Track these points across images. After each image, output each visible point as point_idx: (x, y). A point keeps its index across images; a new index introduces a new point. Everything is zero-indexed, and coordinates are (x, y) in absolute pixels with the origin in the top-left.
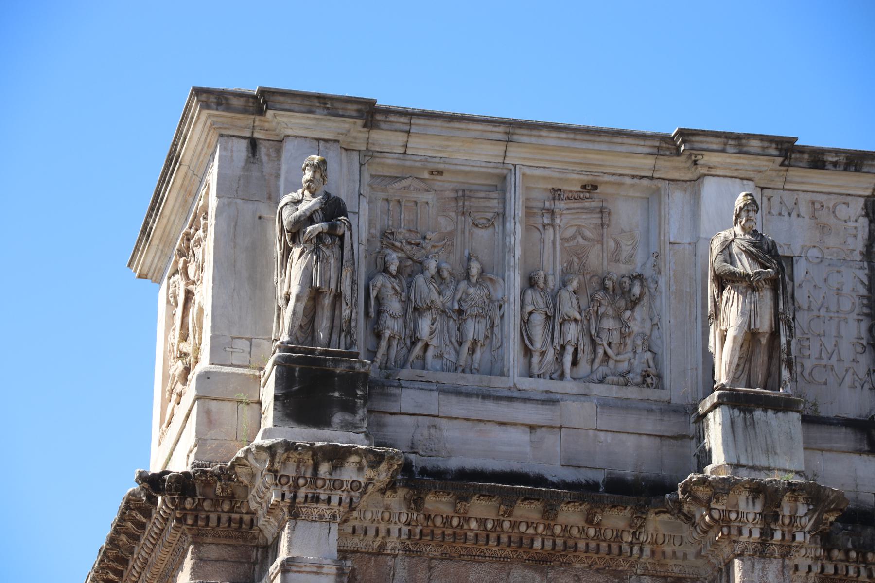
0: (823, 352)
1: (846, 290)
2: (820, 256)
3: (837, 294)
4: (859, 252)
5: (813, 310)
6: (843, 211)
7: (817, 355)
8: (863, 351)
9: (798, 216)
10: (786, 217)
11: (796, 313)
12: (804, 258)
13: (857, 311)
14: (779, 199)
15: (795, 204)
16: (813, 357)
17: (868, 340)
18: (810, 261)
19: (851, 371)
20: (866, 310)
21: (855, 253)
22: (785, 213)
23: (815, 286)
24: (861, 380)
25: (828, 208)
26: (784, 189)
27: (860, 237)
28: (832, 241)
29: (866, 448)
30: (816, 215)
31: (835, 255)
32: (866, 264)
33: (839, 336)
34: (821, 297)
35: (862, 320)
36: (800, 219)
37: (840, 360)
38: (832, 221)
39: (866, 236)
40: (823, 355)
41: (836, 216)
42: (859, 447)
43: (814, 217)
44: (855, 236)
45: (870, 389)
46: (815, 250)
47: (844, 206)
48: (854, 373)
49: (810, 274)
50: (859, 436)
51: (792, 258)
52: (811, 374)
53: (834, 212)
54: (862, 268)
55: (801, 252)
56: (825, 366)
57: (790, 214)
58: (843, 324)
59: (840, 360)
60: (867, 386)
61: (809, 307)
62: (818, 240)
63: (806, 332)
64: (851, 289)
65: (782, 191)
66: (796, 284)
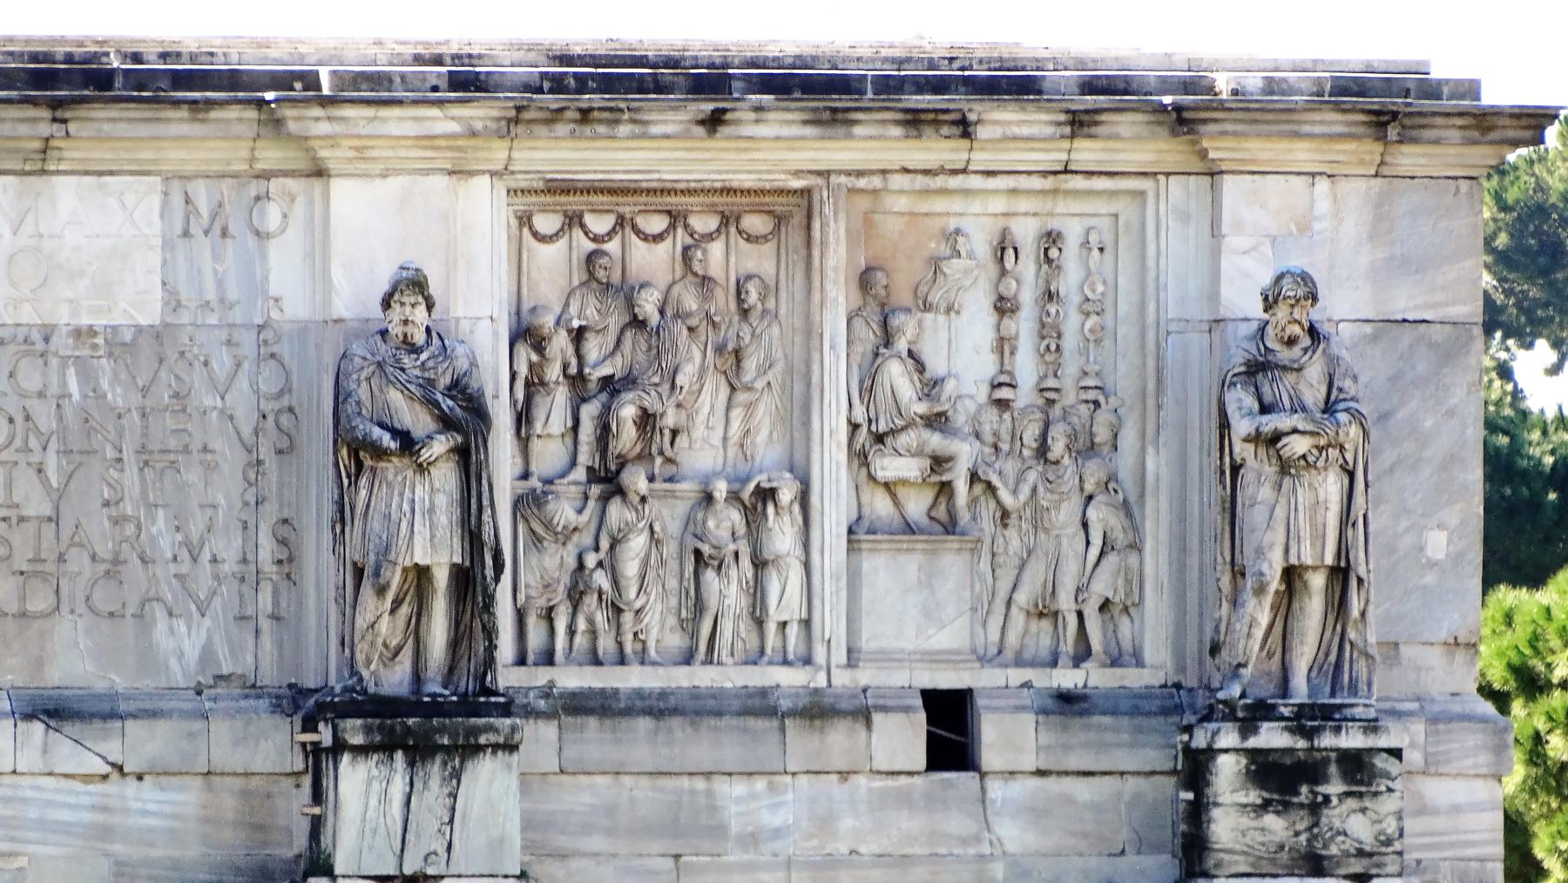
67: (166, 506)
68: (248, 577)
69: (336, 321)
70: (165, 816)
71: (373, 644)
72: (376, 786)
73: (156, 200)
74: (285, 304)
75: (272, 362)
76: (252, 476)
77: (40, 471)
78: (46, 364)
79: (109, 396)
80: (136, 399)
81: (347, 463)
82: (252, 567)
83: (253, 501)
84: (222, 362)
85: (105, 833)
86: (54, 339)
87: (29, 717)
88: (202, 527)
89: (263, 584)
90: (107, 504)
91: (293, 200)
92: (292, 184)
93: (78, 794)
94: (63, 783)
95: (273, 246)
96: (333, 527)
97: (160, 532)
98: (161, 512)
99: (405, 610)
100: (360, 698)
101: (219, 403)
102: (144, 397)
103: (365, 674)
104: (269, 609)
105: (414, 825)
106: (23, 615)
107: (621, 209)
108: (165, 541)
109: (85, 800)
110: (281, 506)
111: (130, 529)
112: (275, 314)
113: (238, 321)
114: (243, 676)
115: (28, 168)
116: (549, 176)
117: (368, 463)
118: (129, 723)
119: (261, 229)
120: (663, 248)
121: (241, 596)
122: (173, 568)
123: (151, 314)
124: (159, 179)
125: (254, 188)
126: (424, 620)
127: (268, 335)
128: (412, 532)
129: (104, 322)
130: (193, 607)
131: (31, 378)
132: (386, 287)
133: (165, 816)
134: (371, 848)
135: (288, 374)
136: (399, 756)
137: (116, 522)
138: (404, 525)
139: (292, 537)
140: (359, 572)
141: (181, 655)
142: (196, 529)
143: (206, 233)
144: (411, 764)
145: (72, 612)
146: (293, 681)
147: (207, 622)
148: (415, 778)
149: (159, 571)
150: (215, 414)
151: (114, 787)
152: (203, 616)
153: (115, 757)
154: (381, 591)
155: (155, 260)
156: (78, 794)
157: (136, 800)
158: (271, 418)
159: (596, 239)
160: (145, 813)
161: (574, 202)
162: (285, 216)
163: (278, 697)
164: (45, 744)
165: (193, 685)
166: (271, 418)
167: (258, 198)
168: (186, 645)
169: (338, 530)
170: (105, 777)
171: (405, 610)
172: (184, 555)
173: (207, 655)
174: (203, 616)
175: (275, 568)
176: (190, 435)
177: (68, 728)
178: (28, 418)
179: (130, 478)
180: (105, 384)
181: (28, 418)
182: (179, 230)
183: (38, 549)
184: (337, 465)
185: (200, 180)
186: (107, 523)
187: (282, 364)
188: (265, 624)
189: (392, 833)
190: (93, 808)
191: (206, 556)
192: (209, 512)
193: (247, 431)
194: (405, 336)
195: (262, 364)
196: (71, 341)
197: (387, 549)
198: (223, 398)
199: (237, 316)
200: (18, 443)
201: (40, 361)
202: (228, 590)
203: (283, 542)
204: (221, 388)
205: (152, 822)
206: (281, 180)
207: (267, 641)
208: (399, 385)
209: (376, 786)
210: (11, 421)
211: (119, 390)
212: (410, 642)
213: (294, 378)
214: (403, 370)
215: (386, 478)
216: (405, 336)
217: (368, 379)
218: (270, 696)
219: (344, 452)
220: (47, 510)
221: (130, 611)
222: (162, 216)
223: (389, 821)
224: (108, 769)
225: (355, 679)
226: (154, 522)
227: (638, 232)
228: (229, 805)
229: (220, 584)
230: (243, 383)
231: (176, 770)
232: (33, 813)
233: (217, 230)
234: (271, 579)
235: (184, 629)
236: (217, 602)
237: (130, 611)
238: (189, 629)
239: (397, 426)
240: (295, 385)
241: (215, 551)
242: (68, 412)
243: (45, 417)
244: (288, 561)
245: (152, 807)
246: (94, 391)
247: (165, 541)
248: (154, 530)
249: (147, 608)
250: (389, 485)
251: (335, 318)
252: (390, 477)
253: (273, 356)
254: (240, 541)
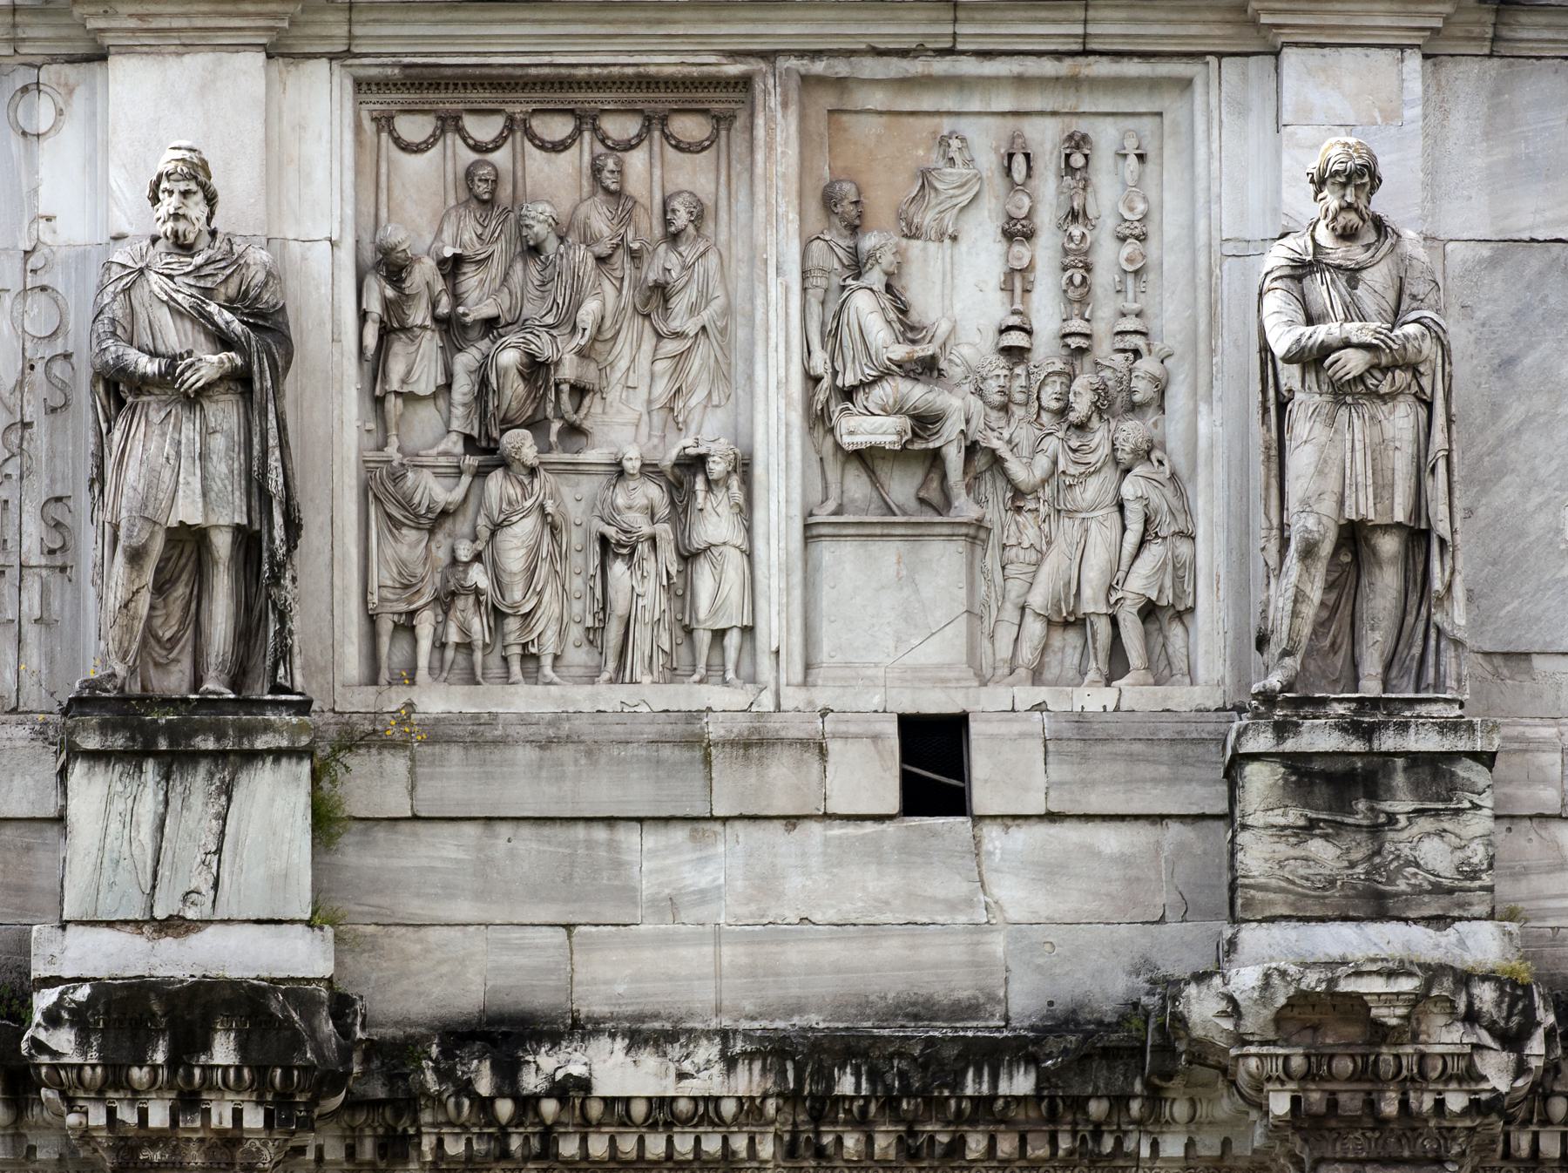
91: (71, 92)
107: (509, 108)
112: (46, 237)
116: (407, 60)
120: (566, 159)
127: (34, 261)
158: (40, 367)
159: (477, 148)
161: (449, 101)
166: (40, 367)
167: (25, 89)
188: (31, 633)
212: (189, 633)
227: (532, 137)
240: (71, 326)
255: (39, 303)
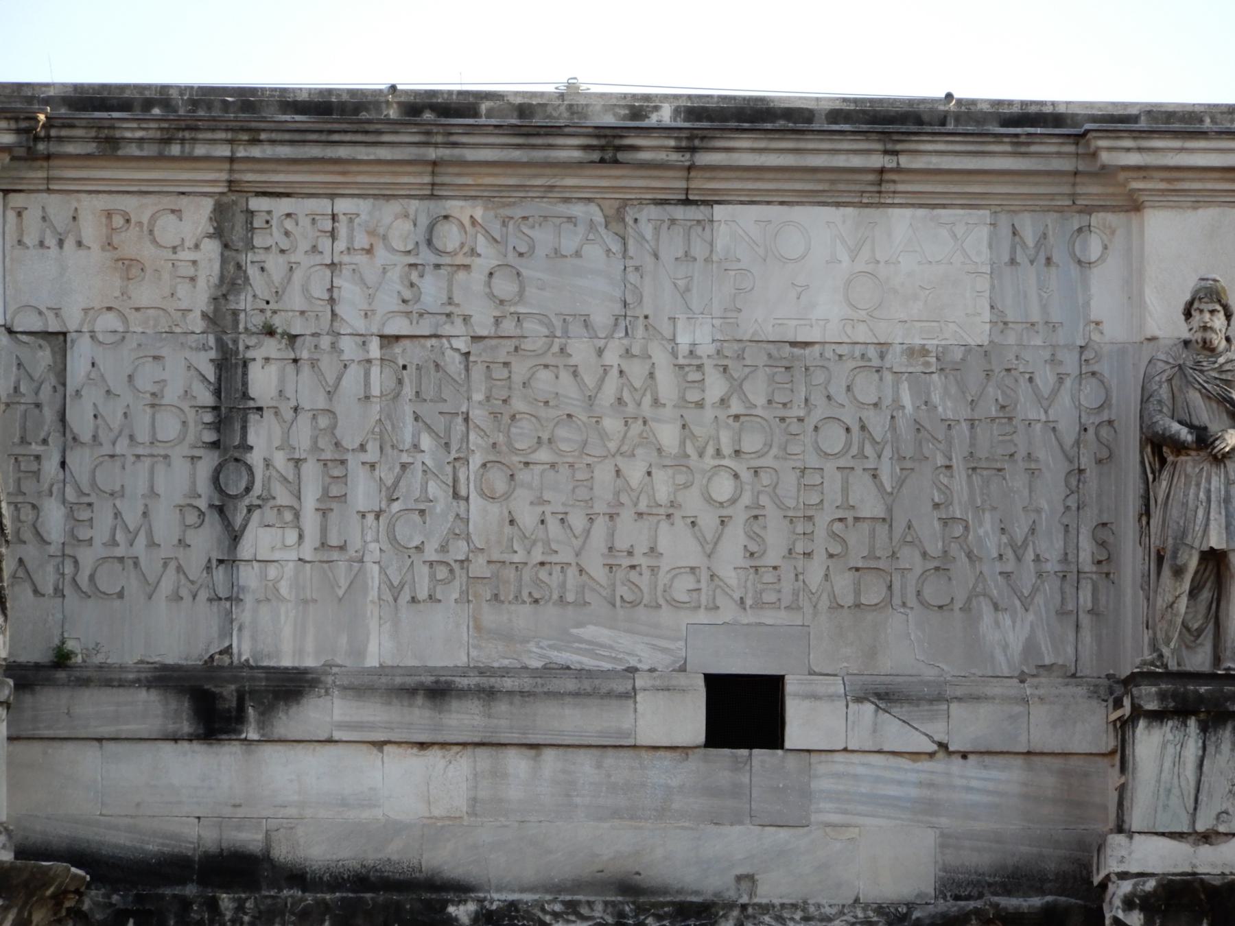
0: (118, 532)
1: (171, 395)
2: (121, 329)
3: (153, 406)
4: (199, 314)
5: (101, 444)
6: (169, 230)
7: (106, 537)
8: (199, 521)
9: (79, 244)
10: (54, 250)
11: (68, 453)
12: (88, 335)
13: (191, 437)
14: (40, 213)
15: (74, 218)
16: (97, 542)
17: (210, 498)
18: (100, 342)
19: (172, 565)
20: (210, 436)
21: (191, 316)
22: (51, 241)
23: (108, 392)
24: (192, 582)
25: (140, 224)
26: (48, 190)
27: (202, 283)
28: (145, 294)
29: (186, 728)
30: (116, 241)
31: (151, 323)
32: (211, 340)
33: (153, 493)
34: (120, 415)
35: (200, 458)
36: (82, 253)
37: (152, 544)
38: (147, 252)
39: (215, 280)
40: (118, 537)
41: (154, 241)
42: (171, 727)
43: (109, 245)
44: (193, 279)
45: (210, 600)
46: (111, 316)
47: (172, 217)
48: (179, 569)
49: (99, 369)
50: (173, 705)
51: (65, 334)
52: (92, 577)
53: (151, 232)
54: (205, 348)
55: (82, 324)
56: (121, 559)
57: (61, 243)
58: (160, 469)
59: (152, 544)
60: (203, 595)
61: (95, 437)
62: (117, 294)
63: (87, 491)
64: (181, 392)
65: (45, 195)
66: (70, 390)
67: (994, 509)
68: (1069, 575)
69: (1149, 340)
70: (989, 792)
71: (1171, 623)
72: (1171, 750)
73: (984, 231)
74: (1105, 327)
75: (1094, 381)
76: (1074, 482)
77: (875, 476)
78: (881, 379)
79: (940, 409)
80: (965, 413)
81: (1151, 459)
82: (1074, 568)
83: (1074, 506)
84: (1045, 379)
85: (930, 807)
86: (889, 357)
87: (859, 700)
88: (1026, 530)
89: (1083, 582)
90: (937, 506)
91: (1113, 232)
92: (1111, 218)
93: (906, 770)
94: (893, 761)
95: (1095, 272)
96: (1140, 520)
97: (986, 533)
98: (987, 515)
99: (1206, 595)
100: (1160, 670)
101: (1043, 418)
102: (973, 410)
103: (1166, 651)
104: (1089, 605)
105: (1206, 785)
106: (858, 605)
108: (986, 533)
109: (913, 777)
110: (1101, 511)
111: (958, 530)
112: (1096, 337)
113: (1062, 343)
114: (1064, 666)
115: (865, 201)
117: (1170, 458)
118: (954, 707)
119: (1082, 259)
121: (1063, 592)
122: (998, 567)
123: (979, 334)
124: (987, 212)
125: (1076, 221)
126: (1223, 604)
127: (1088, 354)
128: (1208, 519)
129: (935, 342)
130: (1018, 603)
131: (867, 389)
132: (1187, 297)
133: (989, 792)
134: (1166, 807)
135: (1108, 392)
136: (1192, 723)
137: (945, 522)
138: (1201, 513)
139: (1111, 539)
140: (1160, 559)
141: (1005, 647)
142: (1020, 532)
143: (1032, 262)
144: (1204, 728)
145: (904, 605)
146: (1112, 672)
147: (1031, 617)
148: (1207, 743)
149: (985, 569)
150: (1038, 426)
151: (939, 766)
152: (1027, 610)
153: (940, 737)
154: (1178, 572)
155: (984, 284)
156: (906, 770)
157: (962, 777)
158: (1091, 431)
160: (969, 789)
162: (1105, 247)
163: (1096, 686)
164: (875, 724)
165: (1016, 674)
166: (1091, 431)
167: (1080, 230)
168: (1011, 638)
169: (1144, 522)
170: (931, 755)
171: (1206, 595)
172: (1009, 554)
173: (1030, 647)
174: (1027, 610)
175: (1094, 569)
176: (1016, 445)
177: (896, 710)
178: (863, 428)
179: (959, 483)
180: (936, 398)
181: (863, 428)
182: (1006, 258)
183: (872, 548)
184: (1142, 463)
185: (1026, 214)
186: (937, 525)
187: (1102, 382)
188: (1085, 620)
189: (1186, 793)
190: (920, 784)
191: (1030, 555)
192: (1033, 516)
193: (1069, 440)
194: (1205, 342)
195: (1084, 382)
196: (904, 359)
197: (1184, 534)
198: (1046, 412)
199: (1061, 338)
200: (854, 450)
201: (876, 376)
202: (1050, 587)
203: (1102, 544)
204: (1045, 403)
205: (975, 797)
206: (1101, 215)
207: (1087, 636)
208: (1197, 386)
209: (1171, 750)
210: (848, 430)
211: (949, 404)
213: (1114, 395)
214: (1202, 372)
215: (1185, 470)
216: (1205, 342)
217: (1170, 380)
218: (1088, 684)
219: (1149, 449)
220: (879, 512)
221: (958, 605)
222: (990, 246)
223: (1183, 783)
224: (934, 747)
225: (1155, 655)
226: (981, 525)
228: (1048, 782)
229: (1043, 583)
230: (1065, 398)
231: (998, 750)
232: (864, 788)
233: (1042, 260)
234: (1091, 579)
235: (1008, 622)
236: (1039, 599)
237: (958, 605)
238: (1014, 622)
239: (1196, 423)
240: (1114, 401)
241: (1038, 552)
242: (901, 423)
243: (878, 424)
244: (1106, 561)
245: (974, 783)
246: (926, 403)
247: (986, 533)
248: (981, 532)
249: (974, 603)
250: (1187, 476)
251: (1149, 337)
252: (1189, 469)
253: (1093, 374)
254: (1062, 543)
255: (1090, 386)
